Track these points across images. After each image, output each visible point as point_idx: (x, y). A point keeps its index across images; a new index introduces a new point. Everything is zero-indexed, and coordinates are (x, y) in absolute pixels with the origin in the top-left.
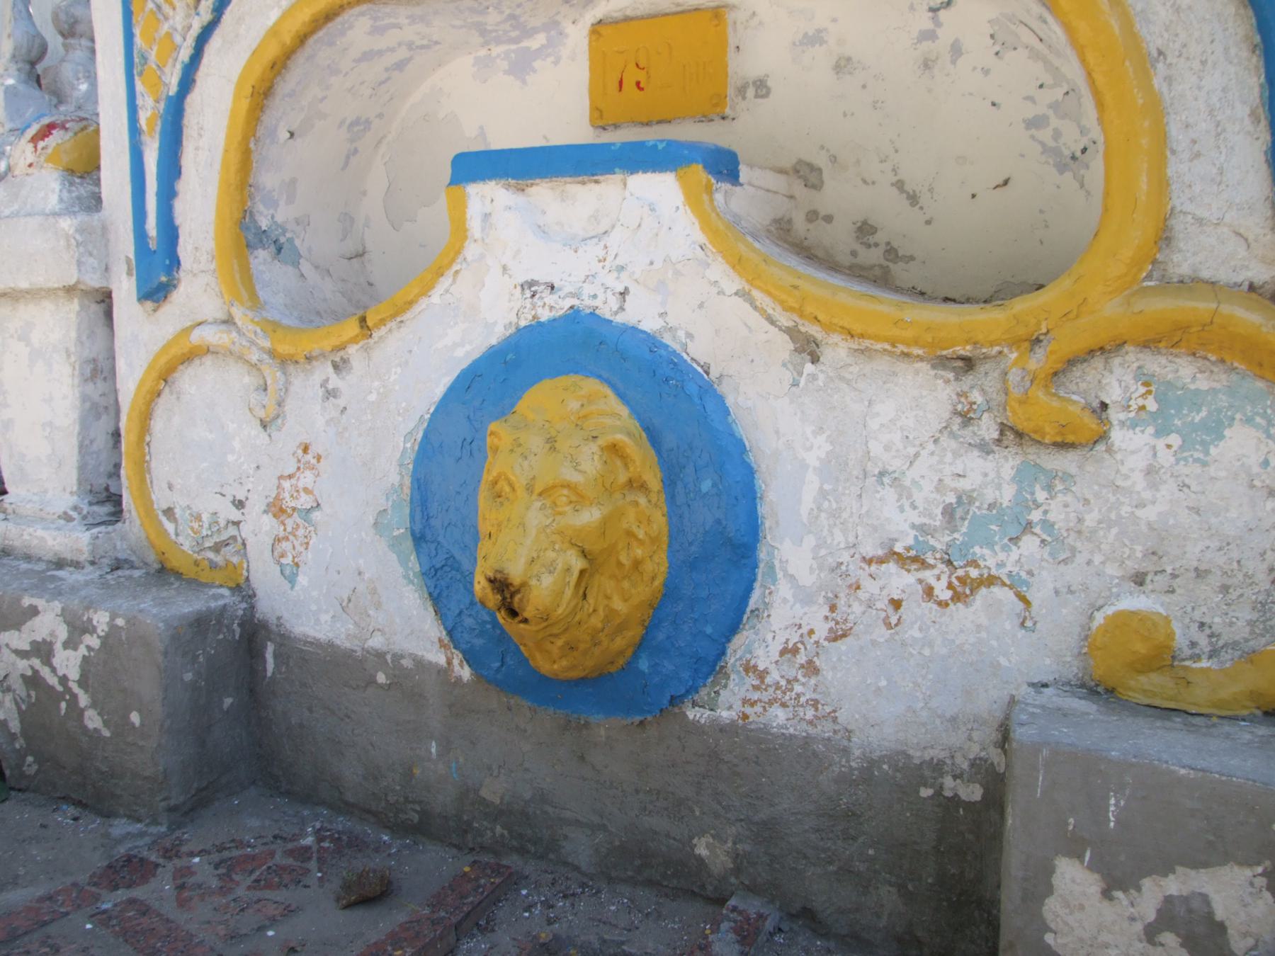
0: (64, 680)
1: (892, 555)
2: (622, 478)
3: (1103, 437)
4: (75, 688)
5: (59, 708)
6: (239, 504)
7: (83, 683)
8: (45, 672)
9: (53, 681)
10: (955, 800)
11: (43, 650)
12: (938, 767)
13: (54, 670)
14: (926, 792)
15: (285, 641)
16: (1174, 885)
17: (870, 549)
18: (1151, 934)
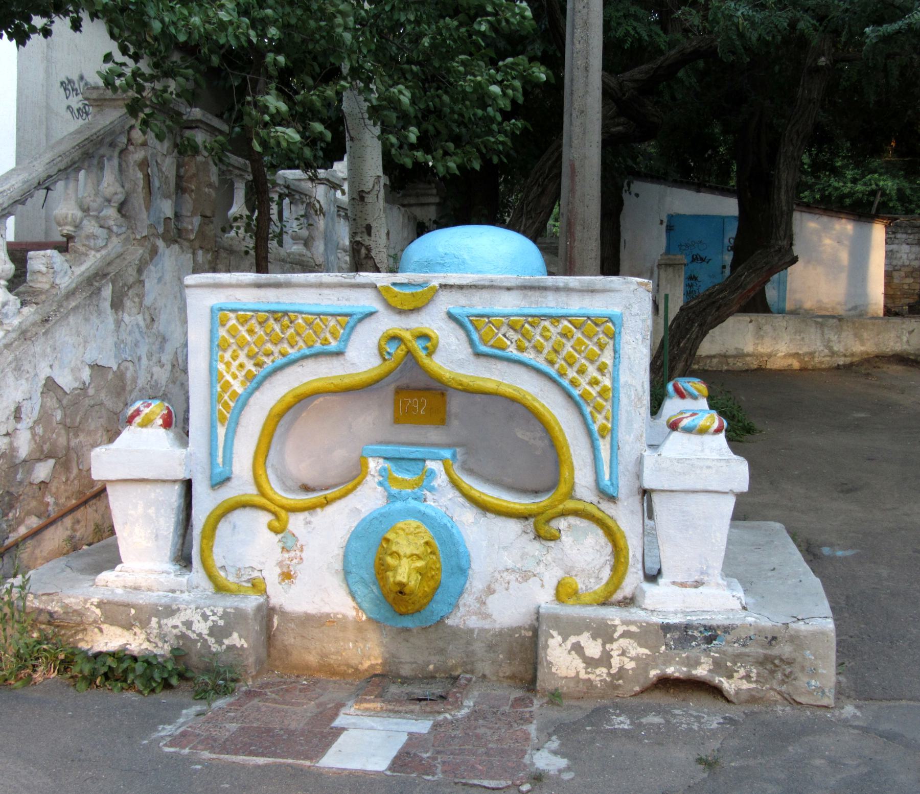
0: (200, 635)
1: (507, 570)
2: (429, 551)
3: (559, 538)
4: (206, 637)
5: (196, 646)
6: (263, 563)
8: (189, 633)
9: (193, 636)
10: (525, 637)
11: (188, 624)
12: (520, 627)
13: (194, 632)
14: (517, 635)
15: (283, 614)
17: (501, 568)
18: (569, 652)
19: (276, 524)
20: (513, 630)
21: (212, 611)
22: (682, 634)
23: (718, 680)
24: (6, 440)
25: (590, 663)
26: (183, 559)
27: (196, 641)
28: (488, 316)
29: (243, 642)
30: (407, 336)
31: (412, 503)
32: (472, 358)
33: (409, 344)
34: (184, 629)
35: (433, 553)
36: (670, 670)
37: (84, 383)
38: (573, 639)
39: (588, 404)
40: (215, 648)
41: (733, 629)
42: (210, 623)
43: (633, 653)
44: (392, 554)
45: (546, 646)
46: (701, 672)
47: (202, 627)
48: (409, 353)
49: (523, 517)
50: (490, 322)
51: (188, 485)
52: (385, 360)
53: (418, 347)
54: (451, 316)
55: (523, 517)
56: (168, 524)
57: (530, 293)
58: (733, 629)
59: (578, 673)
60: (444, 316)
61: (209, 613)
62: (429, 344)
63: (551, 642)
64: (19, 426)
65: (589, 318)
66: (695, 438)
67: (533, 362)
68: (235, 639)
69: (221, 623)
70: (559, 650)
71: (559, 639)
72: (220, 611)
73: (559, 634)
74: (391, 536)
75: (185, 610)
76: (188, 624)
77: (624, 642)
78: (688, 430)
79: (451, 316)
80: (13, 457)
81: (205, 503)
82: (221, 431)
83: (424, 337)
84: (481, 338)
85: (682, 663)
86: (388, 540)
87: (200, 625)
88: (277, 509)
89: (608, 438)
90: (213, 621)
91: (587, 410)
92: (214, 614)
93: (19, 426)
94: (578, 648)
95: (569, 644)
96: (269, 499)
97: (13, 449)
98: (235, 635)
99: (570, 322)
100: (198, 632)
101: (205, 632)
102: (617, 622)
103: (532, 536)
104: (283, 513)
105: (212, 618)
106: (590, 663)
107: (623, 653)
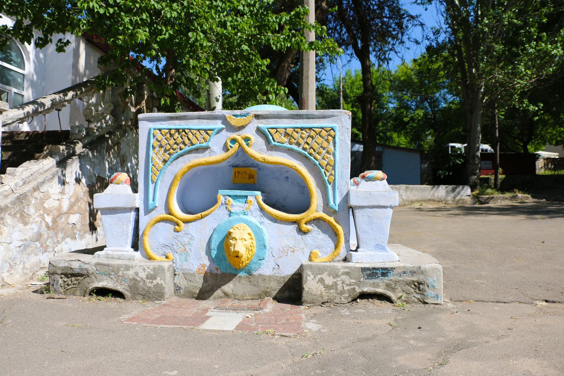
0: (142, 278)
7: (147, 278)
8: (137, 278)
9: (139, 279)
13: (139, 277)
16: (319, 276)
24: (58, 202)
25: (327, 287)
26: (135, 246)
28: (276, 129)
29: (162, 281)
30: (239, 138)
31: (242, 216)
33: (240, 142)
34: (135, 276)
35: (251, 239)
37: (93, 183)
38: (319, 276)
39: (323, 168)
40: (149, 285)
41: (394, 269)
42: (147, 273)
43: (348, 282)
44: (232, 239)
46: (380, 290)
47: (143, 275)
51: (137, 210)
55: (295, 222)
58: (394, 269)
59: (321, 292)
63: (308, 278)
64: (64, 197)
65: (322, 128)
68: (158, 280)
69: (152, 272)
71: (312, 276)
72: (152, 267)
74: (231, 230)
76: (136, 274)
77: (342, 276)
80: (60, 210)
83: (247, 139)
84: (273, 139)
85: (370, 286)
88: (178, 220)
92: (149, 268)
93: (64, 197)
94: (322, 281)
96: (175, 216)
97: (60, 206)
98: (158, 278)
99: (314, 131)
101: (144, 277)
106: (327, 287)
107: (343, 283)
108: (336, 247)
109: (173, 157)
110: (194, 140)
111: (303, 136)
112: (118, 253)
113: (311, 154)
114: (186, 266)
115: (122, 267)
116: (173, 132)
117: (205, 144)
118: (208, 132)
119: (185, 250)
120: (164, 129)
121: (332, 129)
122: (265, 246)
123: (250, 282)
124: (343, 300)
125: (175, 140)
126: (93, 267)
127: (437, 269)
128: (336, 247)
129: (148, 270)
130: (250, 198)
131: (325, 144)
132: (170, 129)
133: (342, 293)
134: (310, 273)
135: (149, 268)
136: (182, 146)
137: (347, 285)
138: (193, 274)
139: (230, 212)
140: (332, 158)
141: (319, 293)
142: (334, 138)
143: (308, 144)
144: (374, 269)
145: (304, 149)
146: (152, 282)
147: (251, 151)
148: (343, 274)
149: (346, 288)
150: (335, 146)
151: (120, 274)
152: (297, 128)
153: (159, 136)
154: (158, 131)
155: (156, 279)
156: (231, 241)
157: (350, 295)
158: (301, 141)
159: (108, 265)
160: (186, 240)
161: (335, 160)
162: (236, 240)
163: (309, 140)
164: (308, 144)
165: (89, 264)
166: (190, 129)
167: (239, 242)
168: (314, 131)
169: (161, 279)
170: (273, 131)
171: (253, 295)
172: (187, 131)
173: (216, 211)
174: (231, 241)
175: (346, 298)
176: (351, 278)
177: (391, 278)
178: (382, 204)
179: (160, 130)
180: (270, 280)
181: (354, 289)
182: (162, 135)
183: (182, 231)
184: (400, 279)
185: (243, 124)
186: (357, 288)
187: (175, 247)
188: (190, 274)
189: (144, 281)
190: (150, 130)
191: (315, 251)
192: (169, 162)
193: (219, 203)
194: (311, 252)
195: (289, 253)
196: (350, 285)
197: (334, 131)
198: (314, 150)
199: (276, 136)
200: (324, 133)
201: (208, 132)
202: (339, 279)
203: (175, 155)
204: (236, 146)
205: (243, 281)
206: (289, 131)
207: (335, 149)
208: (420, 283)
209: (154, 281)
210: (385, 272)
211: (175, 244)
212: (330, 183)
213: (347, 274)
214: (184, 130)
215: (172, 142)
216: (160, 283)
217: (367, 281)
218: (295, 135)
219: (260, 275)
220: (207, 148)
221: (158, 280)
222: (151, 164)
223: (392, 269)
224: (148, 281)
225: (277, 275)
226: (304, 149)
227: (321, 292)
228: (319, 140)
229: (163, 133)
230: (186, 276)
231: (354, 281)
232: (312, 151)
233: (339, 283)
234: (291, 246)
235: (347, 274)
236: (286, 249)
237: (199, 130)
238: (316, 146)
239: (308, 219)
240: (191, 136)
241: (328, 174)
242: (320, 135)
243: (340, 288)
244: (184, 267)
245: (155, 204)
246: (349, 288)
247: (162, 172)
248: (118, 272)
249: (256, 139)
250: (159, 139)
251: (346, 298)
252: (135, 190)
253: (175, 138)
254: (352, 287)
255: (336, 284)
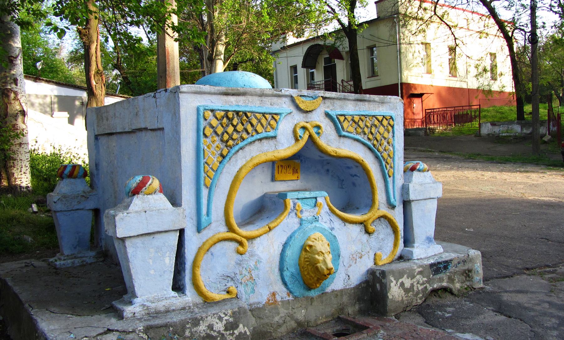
0: (219, 332)
4: (224, 332)
7: (226, 330)
9: (215, 334)
13: (215, 331)
19: (241, 249)
20: (360, 284)
21: (224, 313)
22: (438, 268)
23: (451, 286)
25: (407, 291)
27: (217, 337)
29: (246, 328)
30: (308, 126)
32: (337, 138)
33: (311, 131)
34: (208, 331)
36: (435, 286)
38: (400, 281)
42: (224, 322)
44: (318, 254)
45: (390, 287)
46: (445, 284)
47: (219, 326)
48: (310, 136)
49: (361, 223)
50: (345, 118)
51: (182, 232)
52: (297, 140)
53: (313, 131)
54: (327, 115)
55: (361, 223)
56: (170, 261)
57: (359, 103)
60: (323, 115)
61: (223, 316)
62: (320, 131)
63: (392, 285)
65: (383, 116)
66: (422, 174)
67: (363, 140)
69: (231, 320)
70: (395, 287)
71: (394, 282)
72: (230, 312)
73: (395, 279)
74: (310, 243)
75: (207, 317)
76: (211, 327)
77: (418, 277)
78: (419, 171)
79: (327, 115)
81: (192, 244)
82: (204, 192)
85: (438, 282)
86: (311, 246)
87: (218, 325)
89: (392, 178)
90: (226, 320)
91: (384, 163)
92: (226, 315)
94: (402, 284)
95: (399, 284)
98: (241, 326)
99: (376, 118)
100: (217, 330)
102: (415, 268)
103: (364, 232)
104: (244, 241)
105: (224, 319)
107: (418, 283)
108: (395, 245)
109: (233, 151)
110: (259, 128)
111: (368, 124)
112: (164, 303)
113: (374, 145)
114: (253, 299)
115: (188, 323)
116: (230, 115)
117: (271, 134)
118: (275, 116)
119: (251, 278)
120: (219, 110)
121: (391, 118)
122: (339, 256)
123: (322, 302)
124: (419, 301)
125: (233, 125)
126: (141, 335)
127: (479, 255)
128: (395, 245)
129: (226, 318)
130: (320, 200)
131: (386, 135)
132: (227, 111)
133: (418, 293)
134: (392, 279)
135: (226, 315)
136: (245, 135)
137: (421, 285)
138: (262, 308)
139: (301, 220)
140: (391, 149)
141: (400, 299)
142: (393, 127)
143: (372, 133)
144: (439, 263)
145: (369, 139)
146: (233, 333)
147: (322, 142)
148: (418, 274)
149: (420, 288)
150: (393, 136)
151: (187, 333)
152: (362, 115)
153: (215, 122)
154: (210, 113)
155: (237, 327)
156: (317, 256)
157: (423, 295)
158: (366, 130)
159: (166, 326)
160: (252, 264)
161: (394, 152)
162: (323, 253)
163: (373, 130)
164: (372, 133)
165: (134, 331)
166: (252, 112)
167: (326, 255)
168: (376, 118)
169: (244, 326)
170: (342, 119)
171: (326, 317)
172: (249, 114)
173: (285, 221)
174: (317, 256)
175: (421, 298)
176: (424, 277)
177: (451, 270)
178: (432, 197)
179: (212, 111)
180: (342, 295)
181: (426, 287)
182: (216, 118)
183: (247, 253)
184: (457, 269)
185: (313, 108)
186: (428, 285)
187: (239, 277)
188: (259, 309)
189: (223, 335)
190: (198, 109)
191: (379, 252)
192: (227, 158)
193: (289, 210)
194: (375, 254)
195: (358, 259)
196: (423, 284)
197: (393, 120)
198: (377, 141)
199: (345, 124)
200: (385, 122)
201: (275, 116)
202: (415, 280)
203: (237, 148)
204: (306, 137)
205: (315, 303)
206: (356, 119)
207: (394, 140)
208: (470, 271)
209: (236, 332)
210: (446, 264)
211: (238, 272)
212: (390, 177)
213: (420, 273)
214: (245, 113)
215: (230, 129)
216: (243, 331)
217: (435, 276)
218: (361, 123)
219: (333, 291)
220: (274, 137)
221: (242, 328)
222: (202, 161)
223: (451, 260)
224: (228, 333)
225: (348, 287)
226: (369, 139)
227: (402, 297)
228: (382, 129)
229: (218, 116)
230: (254, 313)
231: (425, 279)
232: (375, 142)
233: (415, 284)
234: (359, 251)
235: (420, 273)
236: (355, 256)
237: (264, 114)
238: (379, 137)
239: (375, 217)
240: (254, 121)
241: (388, 167)
242: (382, 124)
243: (415, 289)
244: (252, 301)
245: (210, 219)
246: (422, 287)
247: (219, 172)
248: (184, 332)
249: (327, 127)
250: (214, 125)
251: (421, 298)
252: (175, 201)
253: (235, 123)
254: (425, 285)
255: (412, 285)
